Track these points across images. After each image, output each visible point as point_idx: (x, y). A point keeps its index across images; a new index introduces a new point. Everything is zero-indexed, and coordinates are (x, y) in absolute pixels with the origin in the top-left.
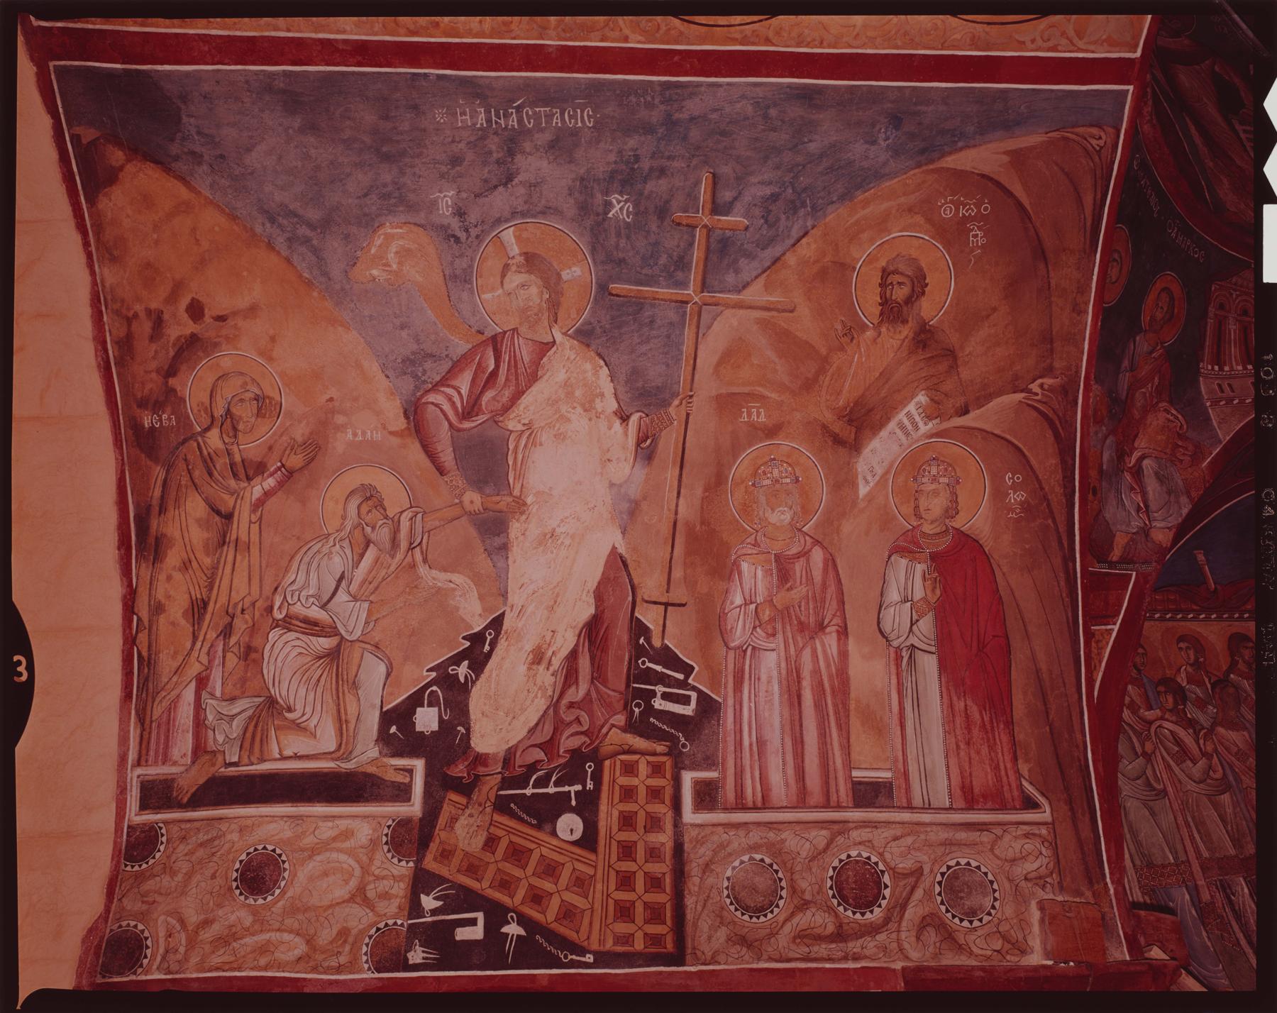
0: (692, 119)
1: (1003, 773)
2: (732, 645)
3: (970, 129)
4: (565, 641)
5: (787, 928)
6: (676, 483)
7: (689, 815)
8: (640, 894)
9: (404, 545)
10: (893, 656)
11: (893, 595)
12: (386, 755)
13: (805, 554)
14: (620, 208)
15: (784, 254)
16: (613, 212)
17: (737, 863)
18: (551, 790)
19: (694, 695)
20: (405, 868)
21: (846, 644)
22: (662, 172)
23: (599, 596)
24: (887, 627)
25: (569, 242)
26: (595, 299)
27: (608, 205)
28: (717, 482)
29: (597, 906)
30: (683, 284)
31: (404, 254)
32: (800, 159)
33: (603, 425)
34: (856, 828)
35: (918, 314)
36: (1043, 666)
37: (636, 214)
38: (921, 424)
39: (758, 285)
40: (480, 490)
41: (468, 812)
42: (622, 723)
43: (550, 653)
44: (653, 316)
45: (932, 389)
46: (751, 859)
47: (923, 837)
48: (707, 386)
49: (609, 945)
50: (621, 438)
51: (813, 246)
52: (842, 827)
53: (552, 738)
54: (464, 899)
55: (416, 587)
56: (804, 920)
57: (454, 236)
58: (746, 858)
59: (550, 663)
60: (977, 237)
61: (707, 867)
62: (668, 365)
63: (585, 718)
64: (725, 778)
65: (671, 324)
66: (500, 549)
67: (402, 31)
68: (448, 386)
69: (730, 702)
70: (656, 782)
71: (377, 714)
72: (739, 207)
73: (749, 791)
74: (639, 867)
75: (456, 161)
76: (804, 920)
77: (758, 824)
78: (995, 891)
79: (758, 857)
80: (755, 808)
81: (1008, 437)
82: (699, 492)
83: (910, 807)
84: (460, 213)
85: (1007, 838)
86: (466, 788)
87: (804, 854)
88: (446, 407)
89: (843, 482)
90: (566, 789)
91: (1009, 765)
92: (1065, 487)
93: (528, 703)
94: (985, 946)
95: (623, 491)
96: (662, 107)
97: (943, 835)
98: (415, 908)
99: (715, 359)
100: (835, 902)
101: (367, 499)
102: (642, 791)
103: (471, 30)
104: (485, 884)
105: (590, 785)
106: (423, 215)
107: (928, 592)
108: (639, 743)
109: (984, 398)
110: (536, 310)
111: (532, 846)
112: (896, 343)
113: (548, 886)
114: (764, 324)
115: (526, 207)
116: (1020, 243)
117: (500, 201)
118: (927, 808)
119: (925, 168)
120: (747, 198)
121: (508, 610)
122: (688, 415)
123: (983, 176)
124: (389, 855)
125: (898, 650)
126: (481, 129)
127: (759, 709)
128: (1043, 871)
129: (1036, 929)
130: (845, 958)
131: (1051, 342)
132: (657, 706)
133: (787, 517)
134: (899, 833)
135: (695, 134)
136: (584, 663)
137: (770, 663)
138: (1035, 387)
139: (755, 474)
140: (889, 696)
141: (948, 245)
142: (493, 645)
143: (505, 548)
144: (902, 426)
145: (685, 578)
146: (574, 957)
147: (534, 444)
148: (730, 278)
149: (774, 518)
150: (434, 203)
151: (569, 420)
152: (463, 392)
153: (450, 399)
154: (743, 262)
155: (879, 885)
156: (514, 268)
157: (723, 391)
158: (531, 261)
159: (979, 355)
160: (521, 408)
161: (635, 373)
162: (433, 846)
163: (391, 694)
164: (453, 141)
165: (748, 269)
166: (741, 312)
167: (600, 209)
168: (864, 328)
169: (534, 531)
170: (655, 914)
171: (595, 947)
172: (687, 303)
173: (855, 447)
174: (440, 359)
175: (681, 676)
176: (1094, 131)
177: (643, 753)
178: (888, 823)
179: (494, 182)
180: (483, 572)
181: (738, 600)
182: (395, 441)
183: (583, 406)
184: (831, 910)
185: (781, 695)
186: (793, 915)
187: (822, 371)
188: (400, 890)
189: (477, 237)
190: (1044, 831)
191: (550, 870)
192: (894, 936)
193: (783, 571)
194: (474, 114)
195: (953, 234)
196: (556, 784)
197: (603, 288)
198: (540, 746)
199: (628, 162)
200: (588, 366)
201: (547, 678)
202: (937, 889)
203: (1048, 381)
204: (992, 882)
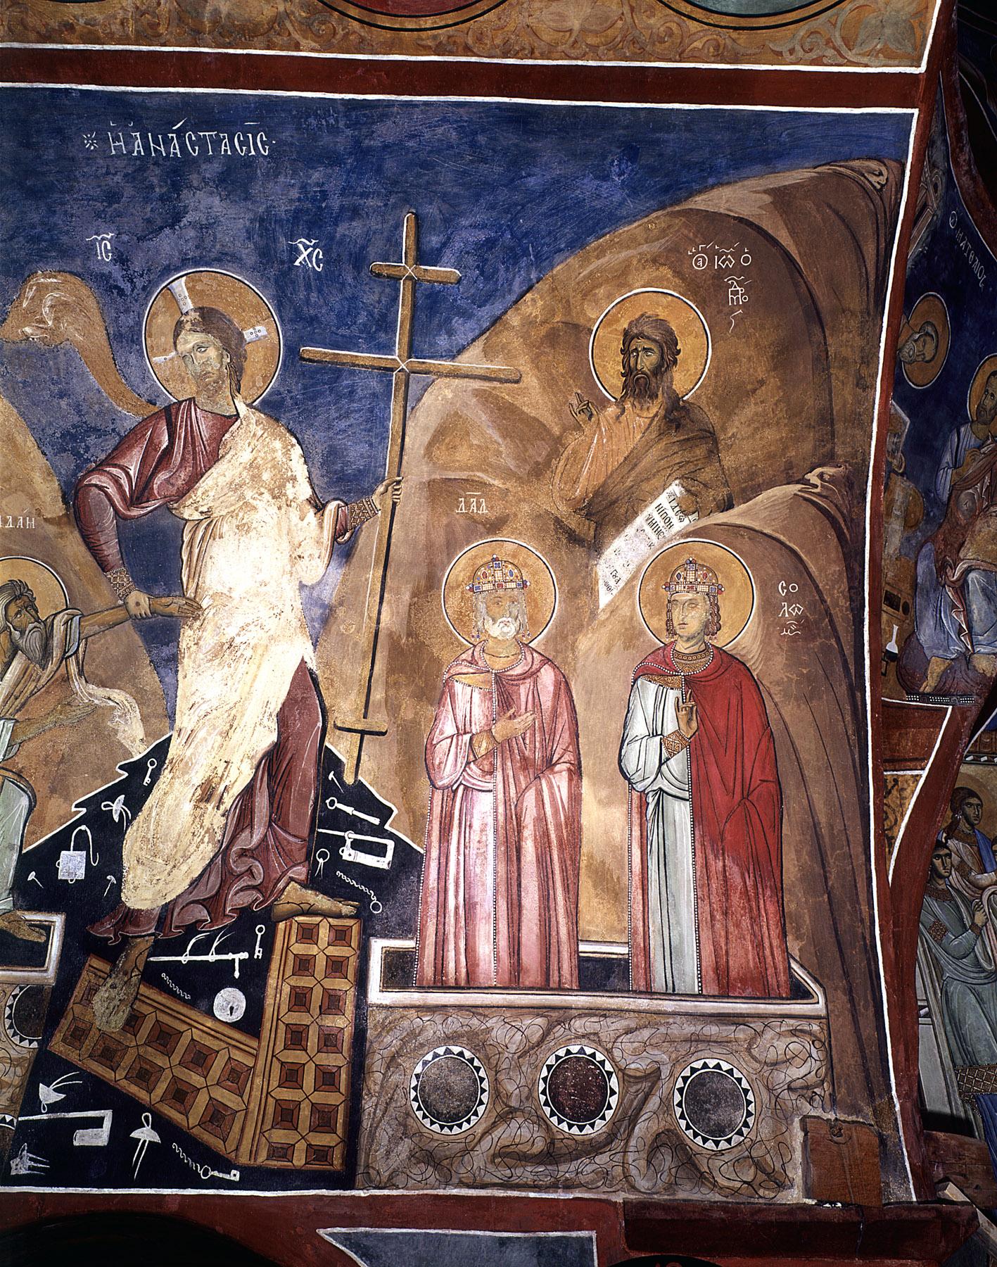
0: (386, 147)
1: (768, 952)
2: (440, 784)
3: (721, 162)
4: (241, 775)
5: (486, 1143)
6: (379, 585)
7: (375, 994)
8: (308, 1093)
9: (57, 653)
10: (636, 802)
11: (639, 727)
12: (21, 908)
14: (308, 254)
15: (505, 313)
16: (301, 259)
17: (429, 1057)
18: (212, 957)
19: (391, 844)
20: (27, 1047)
21: (579, 786)
22: (355, 212)
23: (283, 719)
24: (630, 767)
25: (251, 296)
26: (284, 364)
27: (295, 252)
28: (429, 585)
29: (254, 1106)
31: (60, 308)
32: (517, 197)
33: (294, 514)
34: (580, 1016)
35: (670, 388)
36: (823, 819)
37: (327, 262)
38: (675, 520)
39: (475, 351)
40: (148, 590)
41: (110, 982)
42: (303, 877)
43: (221, 788)
44: (353, 386)
45: (688, 479)
46: (448, 1051)
47: (663, 1030)
48: (417, 471)
50: (313, 532)
51: (540, 303)
52: (562, 1015)
53: (218, 892)
54: (90, 1093)
55: (69, 704)
56: (506, 1134)
57: (116, 287)
58: (441, 1051)
60: (737, 294)
61: (392, 1061)
62: (371, 445)
63: (258, 869)
64: (423, 948)
65: (374, 395)
66: (168, 660)
67: (33, 36)
68: (115, 466)
69: (434, 853)
71: (15, 857)
72: (448, 255)
73: (451, 966)
74: (311, 1059)
75: (113, 196)
76: (506, 1134)
77: (460, 1007)
78: (749, 1103)
79: (456, 1049)
80: (457, 988)
81: (782, 538)
82: (406, 597)
83: (649, 993)
84: (121, 259)
85: (769, 1034)
86: (111, 953)
87: (513, 1048)
88: (112, 490)
89: (580, 588)
90: (230, 956)
91: (775, 943)
92: (851, 600)
93: (192, 849)
94: (733, 1176)
95: (315, 594)
96: (349, 132)
97: (689, 1029)
98: (30, 1102)
99: (427, 439)
100: (547, 1110)
101: (16, 598)
102: (321, 963)
103: (112, 33)
104: (121, 1074)
105: (258, 953)
106: (79, 262)
107: (682, 726)
108: (322, 901)
109: (750, 492)
110: (215, 377)
111: (183, 1027)
112: (643, 422)
113: (196, 1079)
115: (197, 253)
116: (789, 302)
117: (166, 244)
118: (671, 994)
119: (669, 209)
120: (458, 245)
121: (175, 734)
122: (394, 504)
123: (741, 220)
124: (10, 1032)
125: (643, 794)
126: (139, 157)
127: (468, 861)
128: (812, 1078)
129: (798, 1156)
130: (554, 1186)
131: (832, 425)
132: (345, 857)
133: (511, 629)
134: (633, 1025)
135: (391, 166)
136: (262, 802)
137: (484, 809)
138: (813, 477)
139: (474, 576)
140: (630, 851)
141: (702, 304)
142: (155, 776)
143: (172, 662)
144: (651, 522)
145: (386, 702)
146: (216, 1173)
147: (213, 536)
148: (443, 341)
149: (495, 630)
150: (91, 247)
151: (255, 508)
152: (131, 473)
153: (116, 481)
154: (456, 322)
155: (604, 1091)
156: (188, 326)
158: (209, 319)
159: (746, 437)
160: (199, 493)
161: (333, 454)
162: (65, 1023)
163: (33, 833)
164: (108, 173)
167: (285, 257)
168: (604, 403)
169: (209, 639)
170: (323, 1119)
171: (244, 1160)
172: (392, 370)
173: (596, 547)
174: (106, 433)
175: (376, 821)
176: (873, 165)
177: (325, 915)
178: (620, 1011)
179: (159, 222)
180: (147, 688)
181: (450, 729)
182: (51, 529)
183: (271, 491)
185: (496, 847)
186: (494, 1126)
187: (555, 453)
188: (15, 1076)
189: (144, 288)
190: (815, 1028)
191: (200, 1058)
192: (619, 1156)
193: (504, 693)
194: (129, 141)
195: (707, 292)
196: (218, 952)
197: (292, 351)
199: (314, 200)
200: (278, 444)
201: (215, 818)
202: (677, 1098)
203: (829, 471)
204: (746, 1091)
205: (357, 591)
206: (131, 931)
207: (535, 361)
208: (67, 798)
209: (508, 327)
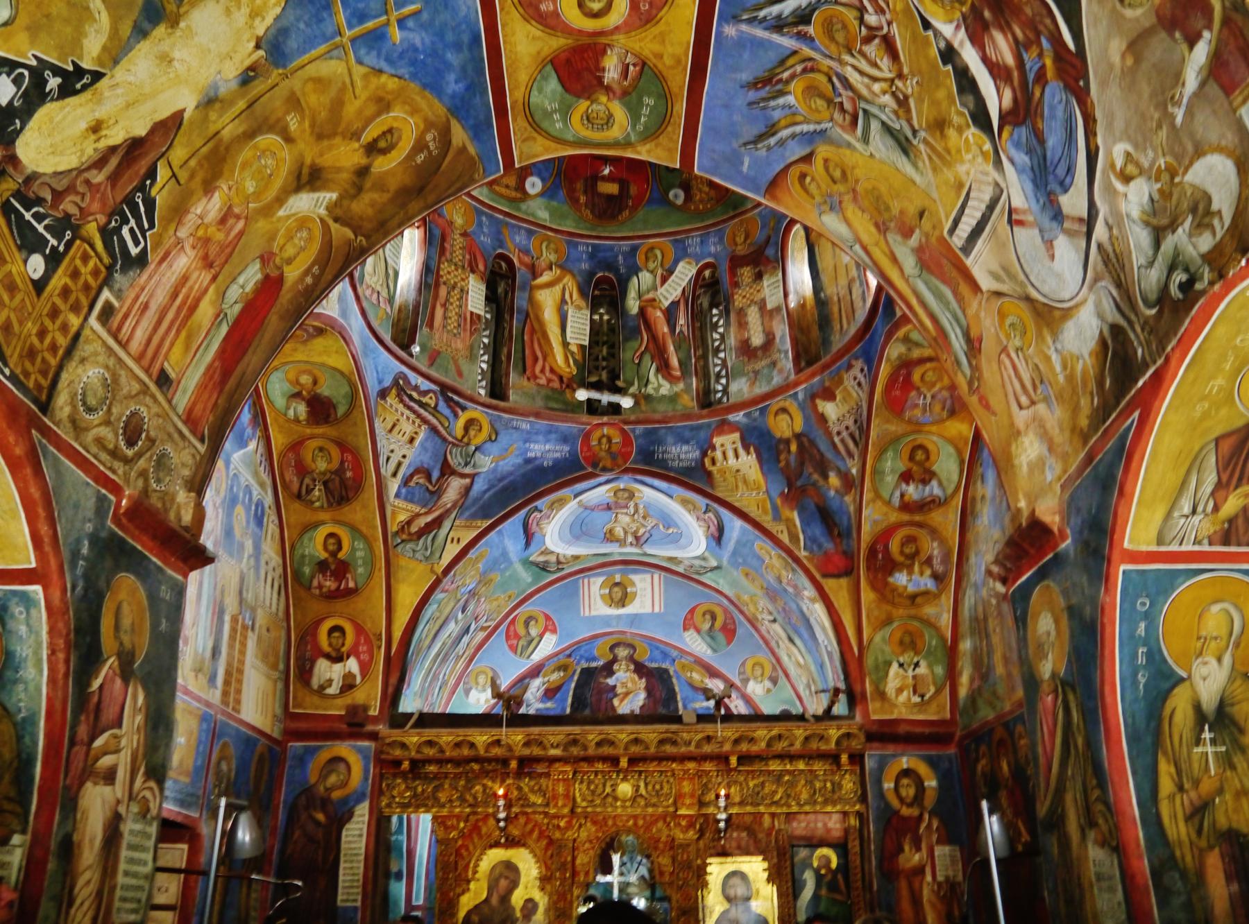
4: (116, 136)
13: (238, 217)
18: (40, 228)
28: (250, 135)
30: (350, 27)
45: (341, 198)
48: (296, 83)
49: (18, 371)
50: (246, 54)
59: (98, 140)
60: (420, 158)
70: (90, 280)
72: (406, 34)
76: (105, 432)
82: (241, 130)
89: (280, 201)
90: (48, 236)
93: (69, 152)
105: (61, 248)
111: (8, 258)
114: (343, 89)
120: (411, 35)
139: (264, 152)
141: (413, 148)
142: (85, 88)
148: (363, 52)
154: (374, 53)
157: (298, 93)
165: (371, 59)
166: (346, 71)
168: (359, 139)
173: (298, 189)
181: (199, 211)
184: (116, 435)
198: (53, 191)
201: (90, 149)
205: (232, 103)
206: (10, 170)
207: (369, 99)
208: (33, 43)
209: (379, 78)
